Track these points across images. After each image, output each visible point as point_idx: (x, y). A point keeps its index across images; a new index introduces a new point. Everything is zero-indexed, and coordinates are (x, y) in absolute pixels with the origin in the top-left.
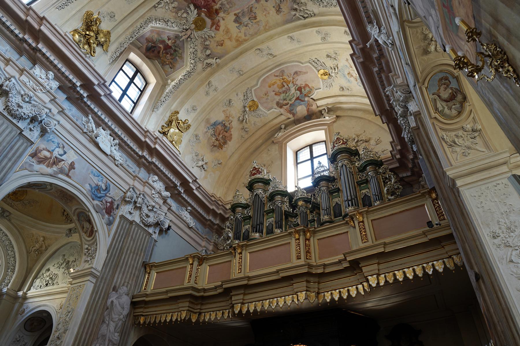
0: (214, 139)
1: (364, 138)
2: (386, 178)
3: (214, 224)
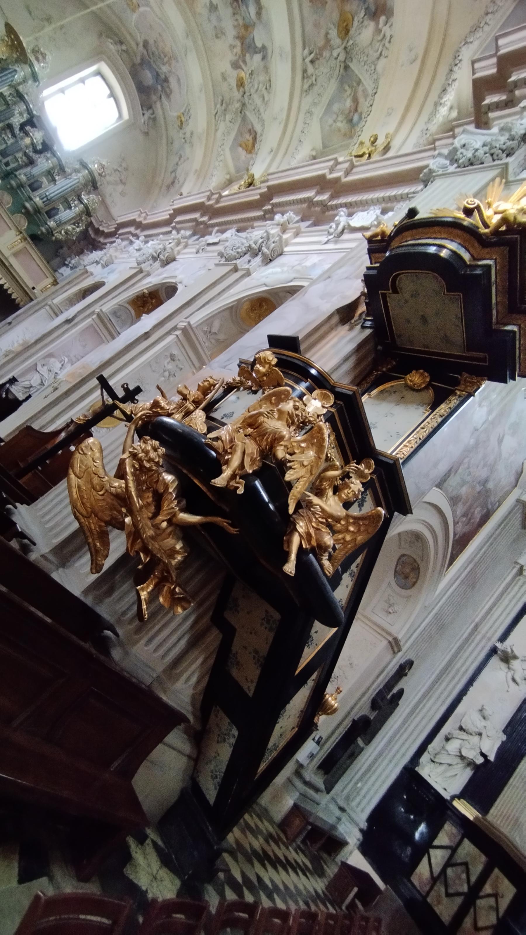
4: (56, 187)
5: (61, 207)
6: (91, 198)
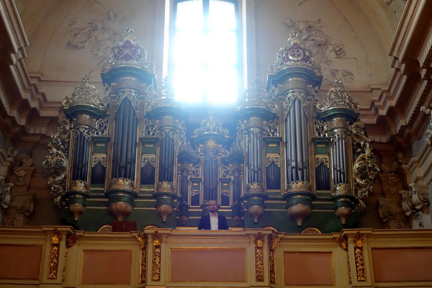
2: (359, 145)
4: (291, 145)
5: (320, 157)
6: (333, 96)
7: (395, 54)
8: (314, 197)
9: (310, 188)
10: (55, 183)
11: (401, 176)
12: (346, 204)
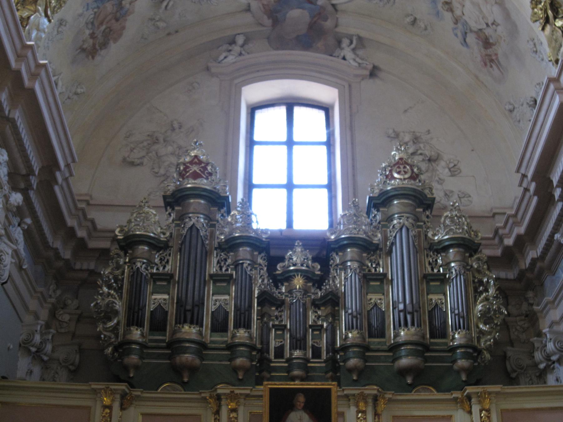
0: (88, 32)
1: (427, 153)
2: (481, 282)
3: (58, 256)
5: (434, 298)
6: (448, 222)
7: (523, 171)
8: (427, 348)
9: (423, 337)
10: (106, 329)
11: (532, 319)
12: (466, 356)
